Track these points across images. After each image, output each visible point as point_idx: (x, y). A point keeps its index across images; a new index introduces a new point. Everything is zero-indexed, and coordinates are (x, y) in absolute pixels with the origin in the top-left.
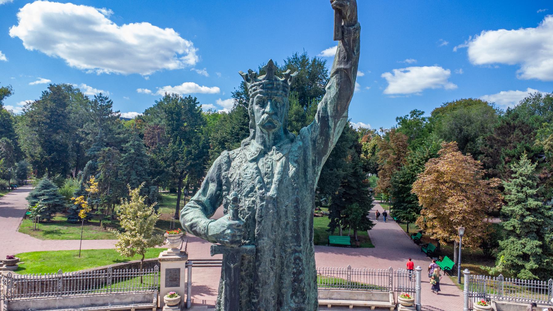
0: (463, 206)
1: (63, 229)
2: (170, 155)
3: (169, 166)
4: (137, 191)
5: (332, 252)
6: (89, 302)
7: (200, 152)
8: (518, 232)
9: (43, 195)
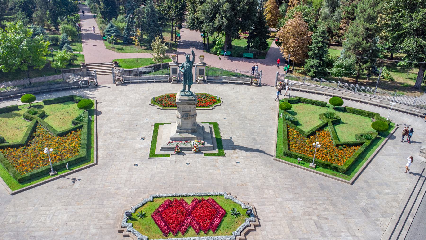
0: (294, 44)
1: (124, 47)
2: (167, 8)
3: (166, 14)
4: (158, 38)
5: (242, 61)
6: (148, 78)
7: (182, 6)
8: (313, 56)
9: (111, 30)
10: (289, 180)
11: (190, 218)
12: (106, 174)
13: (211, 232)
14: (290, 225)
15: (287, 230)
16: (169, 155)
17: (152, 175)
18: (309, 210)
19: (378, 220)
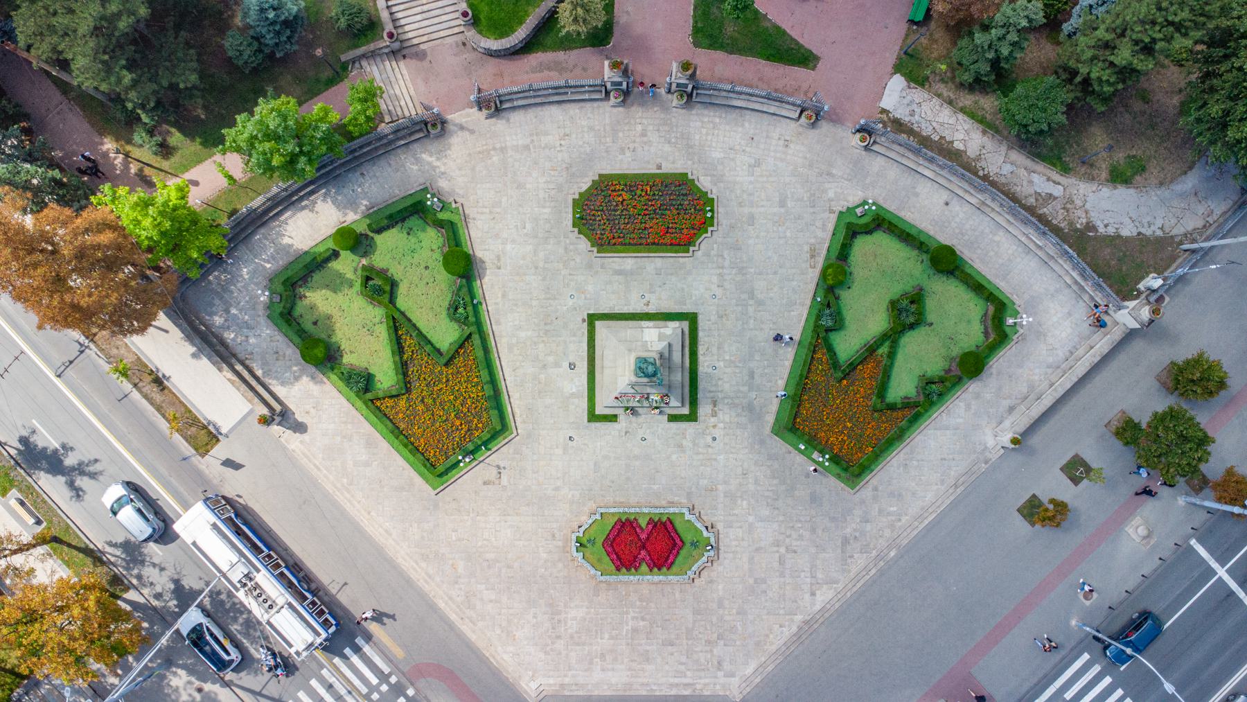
10: (775, 482)
11: (643, 553)
12: (535, 457)
13: (664, 569)
14: (751, 559)
15: (746, 566)
16: (616, 416)
17: (595, 464)
18: (781, 537)
19: (851, 557)
